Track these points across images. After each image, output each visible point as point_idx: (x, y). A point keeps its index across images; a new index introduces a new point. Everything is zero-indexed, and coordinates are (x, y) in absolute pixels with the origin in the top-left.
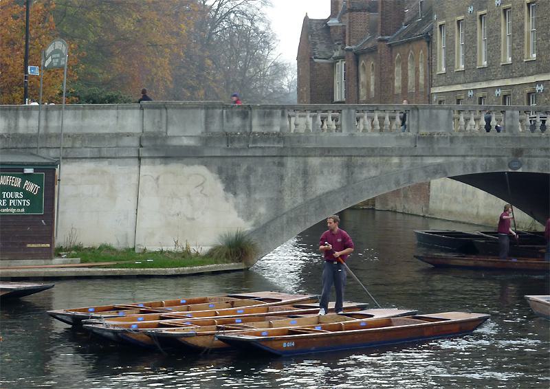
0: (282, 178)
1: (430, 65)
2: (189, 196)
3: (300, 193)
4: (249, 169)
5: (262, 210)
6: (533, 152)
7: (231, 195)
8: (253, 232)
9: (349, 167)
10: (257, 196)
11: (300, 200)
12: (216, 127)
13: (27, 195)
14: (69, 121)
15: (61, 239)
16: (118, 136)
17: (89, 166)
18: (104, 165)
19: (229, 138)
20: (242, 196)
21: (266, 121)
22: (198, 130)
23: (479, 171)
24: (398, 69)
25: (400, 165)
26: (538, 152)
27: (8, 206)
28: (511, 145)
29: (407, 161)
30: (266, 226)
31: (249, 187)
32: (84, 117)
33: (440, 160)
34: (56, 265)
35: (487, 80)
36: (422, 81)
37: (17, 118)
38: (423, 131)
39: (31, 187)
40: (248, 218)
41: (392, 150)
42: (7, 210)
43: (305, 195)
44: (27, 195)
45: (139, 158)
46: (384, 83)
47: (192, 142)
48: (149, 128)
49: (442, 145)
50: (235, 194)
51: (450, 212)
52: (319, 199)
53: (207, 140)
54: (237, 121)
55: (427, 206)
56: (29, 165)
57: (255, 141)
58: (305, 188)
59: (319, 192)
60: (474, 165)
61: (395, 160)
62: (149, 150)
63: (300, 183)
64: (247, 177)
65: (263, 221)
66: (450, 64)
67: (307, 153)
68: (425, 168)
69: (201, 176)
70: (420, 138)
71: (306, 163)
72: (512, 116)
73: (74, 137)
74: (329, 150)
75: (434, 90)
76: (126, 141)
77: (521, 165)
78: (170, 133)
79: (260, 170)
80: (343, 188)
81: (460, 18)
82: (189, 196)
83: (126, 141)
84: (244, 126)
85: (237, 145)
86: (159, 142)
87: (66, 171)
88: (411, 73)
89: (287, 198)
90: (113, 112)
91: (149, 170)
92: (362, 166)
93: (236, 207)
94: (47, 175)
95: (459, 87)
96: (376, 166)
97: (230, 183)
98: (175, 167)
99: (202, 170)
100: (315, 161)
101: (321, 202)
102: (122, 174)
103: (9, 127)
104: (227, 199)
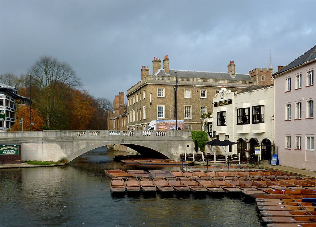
0: (73, 146)
1: (127, 121)
2: (53, 150)
3: (77, 149)
4: (66, 144)
5: (69, 152)
6: (126, 140)
7: (62, 149)
8: (68, 157)
9: (87, 143)
10: (68, 150)
11: (77, 150)
12: (59, 135)
13: (15, 150)
14: (27, 134)
15: (23, 159)
16: (38, 137)
17: (32, 144)
18: (35, 144)
19: (62, 138)
20: (64, 150)
21: (70, 134)
25: (98, 143)
26: (127, 140)
29: (100, 142)
30: (70, 156)
31: (66, 148)
32: (30, 134)
33: (107, 141)
34: (22, 165)
37: (16, 134)
39: (16, 149)
40: (66, 154)
41: (96, 140)
43: (78, 149)
44: (15, 150)
45: (42, 142)
47: (53, 139)
48: (44, 136)
49: (107, 138)
50: (63, 149)
52: (81, 150)
53: (57, 138)
54: (63, 134)
56: (15, 144)
57: (67, 138)
58: (78, 148)
59: (81, 149)
60: (114, 142)
61: (97, 142)
62: (44, 140)
64: (66, 146)
65: (69, 155)
67: (79, 140)
68: (103, 143)
69: (56, 145)
71: (78, 143)
72: (122, 132)
74: (83, 140)
76: (39, 139)
78: (49, 137)
79: (68, 144)
80: (86, 148)
82: (53, 150)
83: (39, 139)
85: (63, 139)
86: (46, 139)
89: (74, 150)
90: (36, 133)
91: (45, 145)
92: (90, 143)
93: (63, 152)
94: (19, 146)
96: (93, 143)
97: (62, 147)
98: (50, 144)
99: (56, 144)
100: (80, 142)
101: (81, 150)
103: (14, 136)
104: (61, 150)
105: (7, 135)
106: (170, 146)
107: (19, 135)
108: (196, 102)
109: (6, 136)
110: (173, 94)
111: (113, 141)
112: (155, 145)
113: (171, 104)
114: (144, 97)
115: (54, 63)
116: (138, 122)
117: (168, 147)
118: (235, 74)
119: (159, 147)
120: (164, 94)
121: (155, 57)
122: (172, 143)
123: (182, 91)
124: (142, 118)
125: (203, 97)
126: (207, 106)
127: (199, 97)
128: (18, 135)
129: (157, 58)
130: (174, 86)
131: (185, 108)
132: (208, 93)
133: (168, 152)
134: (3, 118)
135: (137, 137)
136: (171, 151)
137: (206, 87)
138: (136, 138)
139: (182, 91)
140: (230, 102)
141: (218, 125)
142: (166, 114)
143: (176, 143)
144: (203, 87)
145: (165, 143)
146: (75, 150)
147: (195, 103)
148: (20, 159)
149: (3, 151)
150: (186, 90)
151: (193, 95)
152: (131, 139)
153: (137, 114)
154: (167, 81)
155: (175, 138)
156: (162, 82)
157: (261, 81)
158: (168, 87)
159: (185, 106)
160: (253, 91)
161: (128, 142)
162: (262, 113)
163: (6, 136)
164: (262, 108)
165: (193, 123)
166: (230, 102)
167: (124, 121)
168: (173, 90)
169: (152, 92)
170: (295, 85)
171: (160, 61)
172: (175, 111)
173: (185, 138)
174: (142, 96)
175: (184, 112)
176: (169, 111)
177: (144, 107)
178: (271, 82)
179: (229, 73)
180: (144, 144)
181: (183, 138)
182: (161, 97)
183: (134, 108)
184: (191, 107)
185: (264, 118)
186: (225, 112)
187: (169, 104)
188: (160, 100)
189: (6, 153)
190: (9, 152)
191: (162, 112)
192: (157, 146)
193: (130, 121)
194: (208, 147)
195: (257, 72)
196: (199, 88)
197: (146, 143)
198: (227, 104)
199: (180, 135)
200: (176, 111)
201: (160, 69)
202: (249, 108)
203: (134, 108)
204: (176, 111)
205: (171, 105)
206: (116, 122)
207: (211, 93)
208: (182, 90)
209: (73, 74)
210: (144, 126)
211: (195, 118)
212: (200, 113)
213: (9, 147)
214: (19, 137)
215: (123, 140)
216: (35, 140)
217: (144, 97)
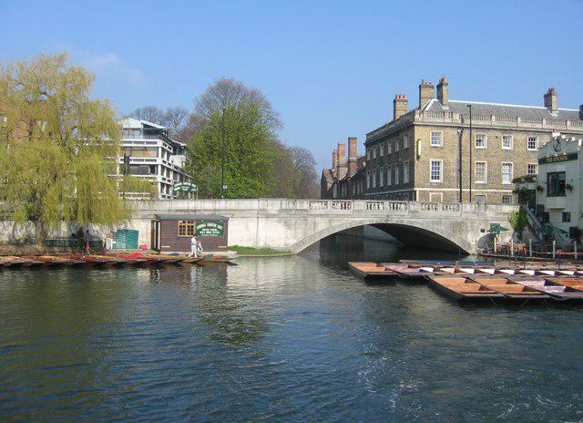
1: (365, 185)
5: (300, 235)
12: (284, 207)
13: (218, 230)
14: (232, 204)
15: (230, 244)
20: (293, 231)
22: (278, 208)
39: (220, 227)
44: (218, 230)
53: (282, 210)
54: (291, 206)
63: (313, 227)
66: (371, 186)
73: (235, 210)
76: (252, 212)
79: (299, 222)
91: (262, 222)
94: (224, 222)
97: (287, 224)
100: (318, 219)
102: (252, 224)
110: (457, 140)
114: (406, 146)
115: (238, 89)
116: (390, 188)
125: (506, 148)
127: (499, 146)
128: (222, 205)
129: (428, 80)
130: (459, 127)
132: (515, 140)
137: (511, 130)
140: (573, 157)
144: (504, 130)
146: (310, 233)
153: (389, 175)
154: (448, 120)
156: (439, 121)
158: (448, 130)
166: (573, 157)
174: (402, 144)
180: (421, 224)
186: (564, 172)
200: (460, 171)
201: (433, 100)
204: (460, 171)
205: (453, 159)
213: (209, 225)
216: (244, 214)
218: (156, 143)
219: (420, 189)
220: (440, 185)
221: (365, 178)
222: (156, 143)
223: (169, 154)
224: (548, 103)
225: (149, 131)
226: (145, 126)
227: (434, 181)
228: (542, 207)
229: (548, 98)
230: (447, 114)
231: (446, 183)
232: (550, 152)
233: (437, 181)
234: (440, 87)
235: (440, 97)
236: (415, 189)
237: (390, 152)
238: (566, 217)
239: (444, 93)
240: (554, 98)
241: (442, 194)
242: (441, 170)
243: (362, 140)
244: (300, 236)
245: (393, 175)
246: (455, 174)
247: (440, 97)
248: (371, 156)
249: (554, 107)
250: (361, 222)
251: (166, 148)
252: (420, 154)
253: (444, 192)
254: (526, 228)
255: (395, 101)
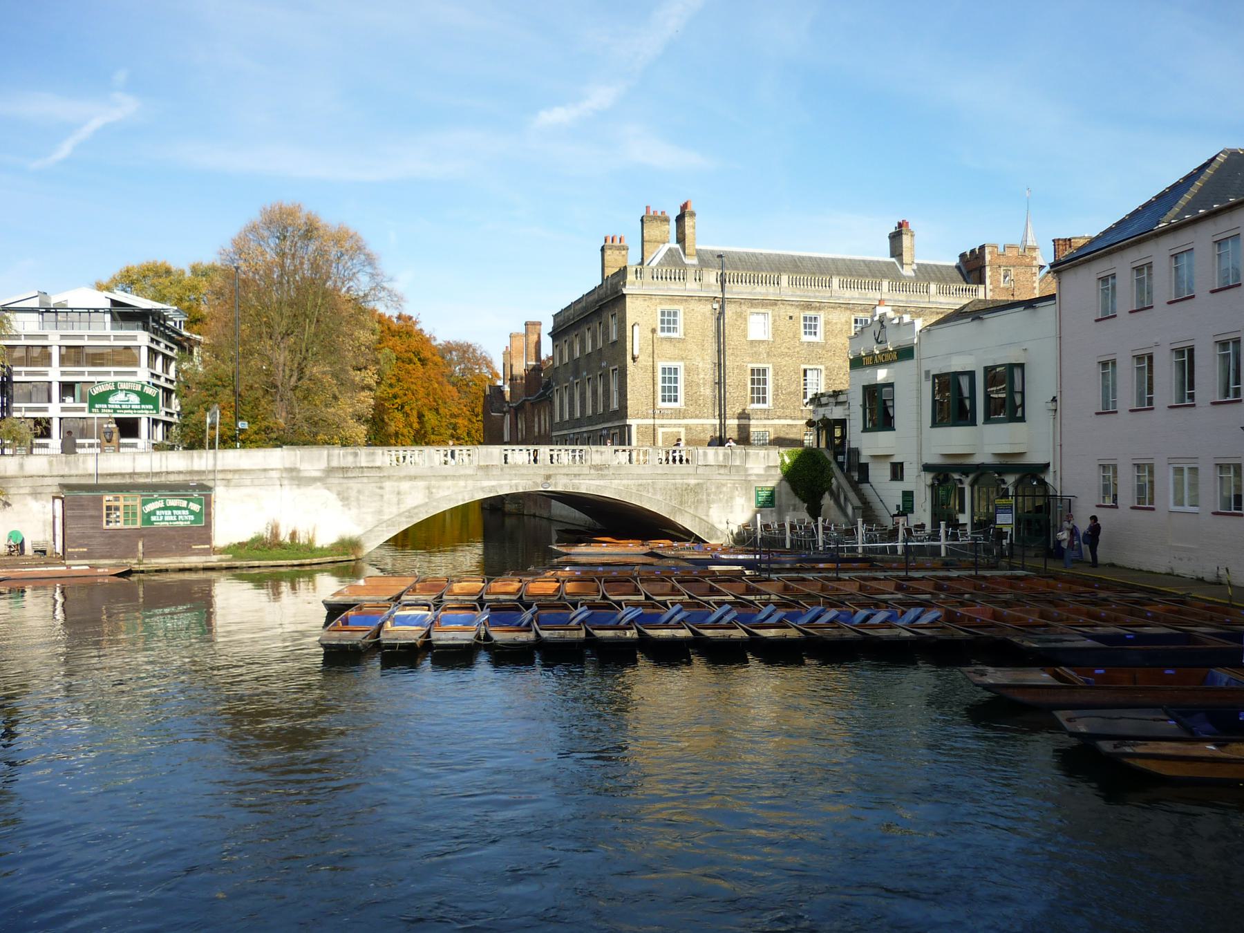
1: (552, 417)
12: (335, 464)
13: (192, 512)
19: (344, 469)
22: (323, 464)
23: (521, 490)
24: (536, 419)
25: (465, 487)
27: (178, 520)
28: (543, 472)
33: (493, 483)
34: (214, 560)
35: (579, 427)
36: (547, 428)
38: (482, 463)
39: (195, 507)
42: (177, 523)
44: (192, 512)
46: (529, 428)
47: (318, 474)
51: (561, 516)
53: (330, 471)
54: (350, 459)
55: (550, 511)
60: (517, 486)
68: (483, 489)
70: (480, 468)
75: (554, 434)
77: (550, 486)
78: (302, 468)
81: (566, 385)
84: (355, 462)
86: (294, 474)
87: (222, 497)
88: (543, 422)
92: (439, 487)
95: (565, 432)
100: (405, 486)
105: (164, 459)
106: (704, 497)
107: (203, 461)
108: (786, 355)
109: (161, 467)
110: (711, 325)
111: (514, 482)
112: (655, 494)
113: (703, 359)
114: (614, 337)
116: (592, 420)
117: (700, 501)
118: (913, 262)
119: (671, 500)
120: (680, 325)
121: (648, 208)
122: (713, 490)
123: (740, 316)
124: (607, 405)
126: (822, 367)
128: (202, 460)
129: (657, 208)
131: (749, 372)
132: (827, 323)
133: (700, 518)
134: (151, 407)
135: (598, 468)
136: (707, 516)
138: (593, 471)
139: (740, 316)
140: (905, 353)
141: (865, 430)
142: (686, 394)
143: (724, 489)
144: (808, 306)
145: (688, 489)
146: (390, 511)
147: (783, 355)
148: (208, 539)
149: (153, 513)
150: (752, 313)
151: (776, 330)
152: (575, 475)
153: (589, 394)
154: (691, 286)
155: (722, 471)
157: (1002, 285)
158: (693, 305)
159: (750, 366)
160: (985, 316)
161: (565, 486)
162: (1018, 387)
163: (161, 467)
164: (1017, 373)
165: (776, 422)
166: (905, 353)
167: (542, 417)
168: (708, 314)
169: (638, 320)
170: (1162, 286)
171: (667, 220)
172: (716, 383)
173: (756, 471)
174: (606, 334)
175: (746, 385)
176: (698, 385)
177: (613, 370)
178: (1034, 288)
179: (893, 260)
181: (750, 472)
182: (670, 339)
183: (576, 373)
184: (771, 369)
185: (1023, 405)
186: (891, 385)
187: (699, 359)
188: (666, 346)
189: (163, 521)
190: (171, 518)
191: (673, 385)
192: (661, 498)
193: (561, 416)
194: (832, 502)
195: (988, 257)
196: (797, 306)
197: (627, 487)
198: (893, 361)
199: (738, 463)
201: (667, 246)
202: (971, 375)
203: (576, 373)
206: (514, 420)
207: (836, 323)
208: (741, 316)
209: (370, 260)
210: (612, 432)
211: (783, 407)
212: (802, 391)
213: (172, 502)
214: (203, 468)
215: (548, 477)
217: (614, 337)
218: (134, 338)
219: (640, 422)
220: (679, 414)
221: (552, 402)
222: (134, 338)
223: (167, 360)
224: (896, 251)
225: (123, 315)
226: (115, 303)
227: (667, 405)
228: (856, 452)
229: (896, 238)
230: (691, 274)
231: (691, 409)
232: (869, 346)
233: (672, 405)
234: (680, 219)
235: (681, 239)
236: (628, 422)
237: (577, 354)
238: (897, 471)
239: (688, 231)
240: (906, 240)
241: (682, 430)
242: (681, 385)
243: (548, 326)
244: (370, 520)
245: (595, 393)
246: (707, 391)
247: (681, 239)
248: (561, 359)
249: (906, 258)
250: (492, 488)
251: (161, 348)
252: (636, 353)
253: (688, 428)
254: (827, 495)
255: (603, 249)
